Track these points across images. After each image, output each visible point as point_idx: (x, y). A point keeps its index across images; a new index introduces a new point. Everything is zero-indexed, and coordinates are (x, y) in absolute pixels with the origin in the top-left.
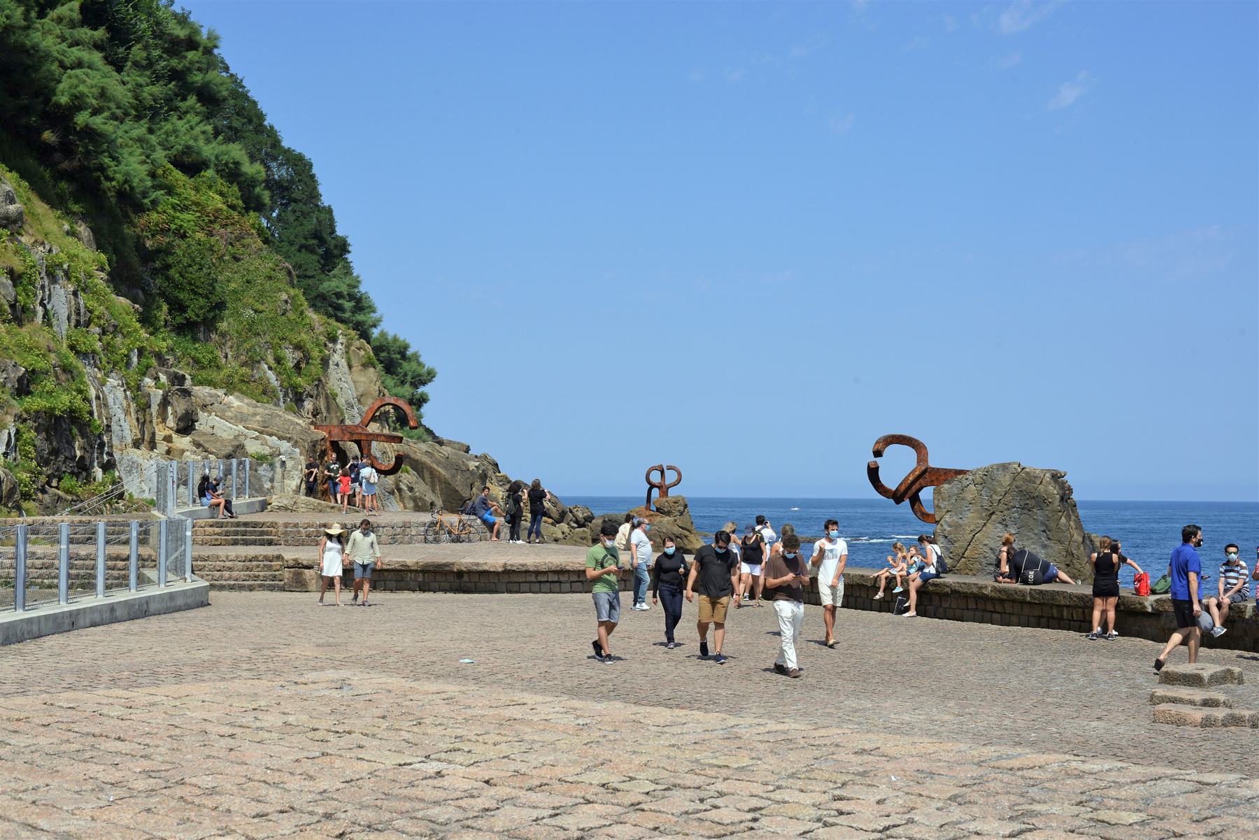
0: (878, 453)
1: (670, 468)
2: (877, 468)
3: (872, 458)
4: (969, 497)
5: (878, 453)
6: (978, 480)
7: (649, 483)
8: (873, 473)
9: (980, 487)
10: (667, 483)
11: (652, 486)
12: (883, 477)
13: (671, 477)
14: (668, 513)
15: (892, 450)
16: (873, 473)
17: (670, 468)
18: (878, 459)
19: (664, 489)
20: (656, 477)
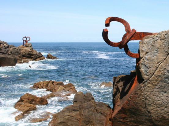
0: (107, 25)
1: (28, 37)
2: (108, 32)
3: (105, 27)
4: (157, 45)
5: (107, 25)
6: (162, 37)
7: (23, 40)
8: (105, 34)
9: (163, 41)
10: (27, 40)
11: (24, 41)
12: (111, 38)
13: (28, 39)
14: (27, 47)
15: (112, 23)
16: (105, 34)
17: (28, 37)
18: (107, 28)
19: (26, 42)
20: (25, 39)
